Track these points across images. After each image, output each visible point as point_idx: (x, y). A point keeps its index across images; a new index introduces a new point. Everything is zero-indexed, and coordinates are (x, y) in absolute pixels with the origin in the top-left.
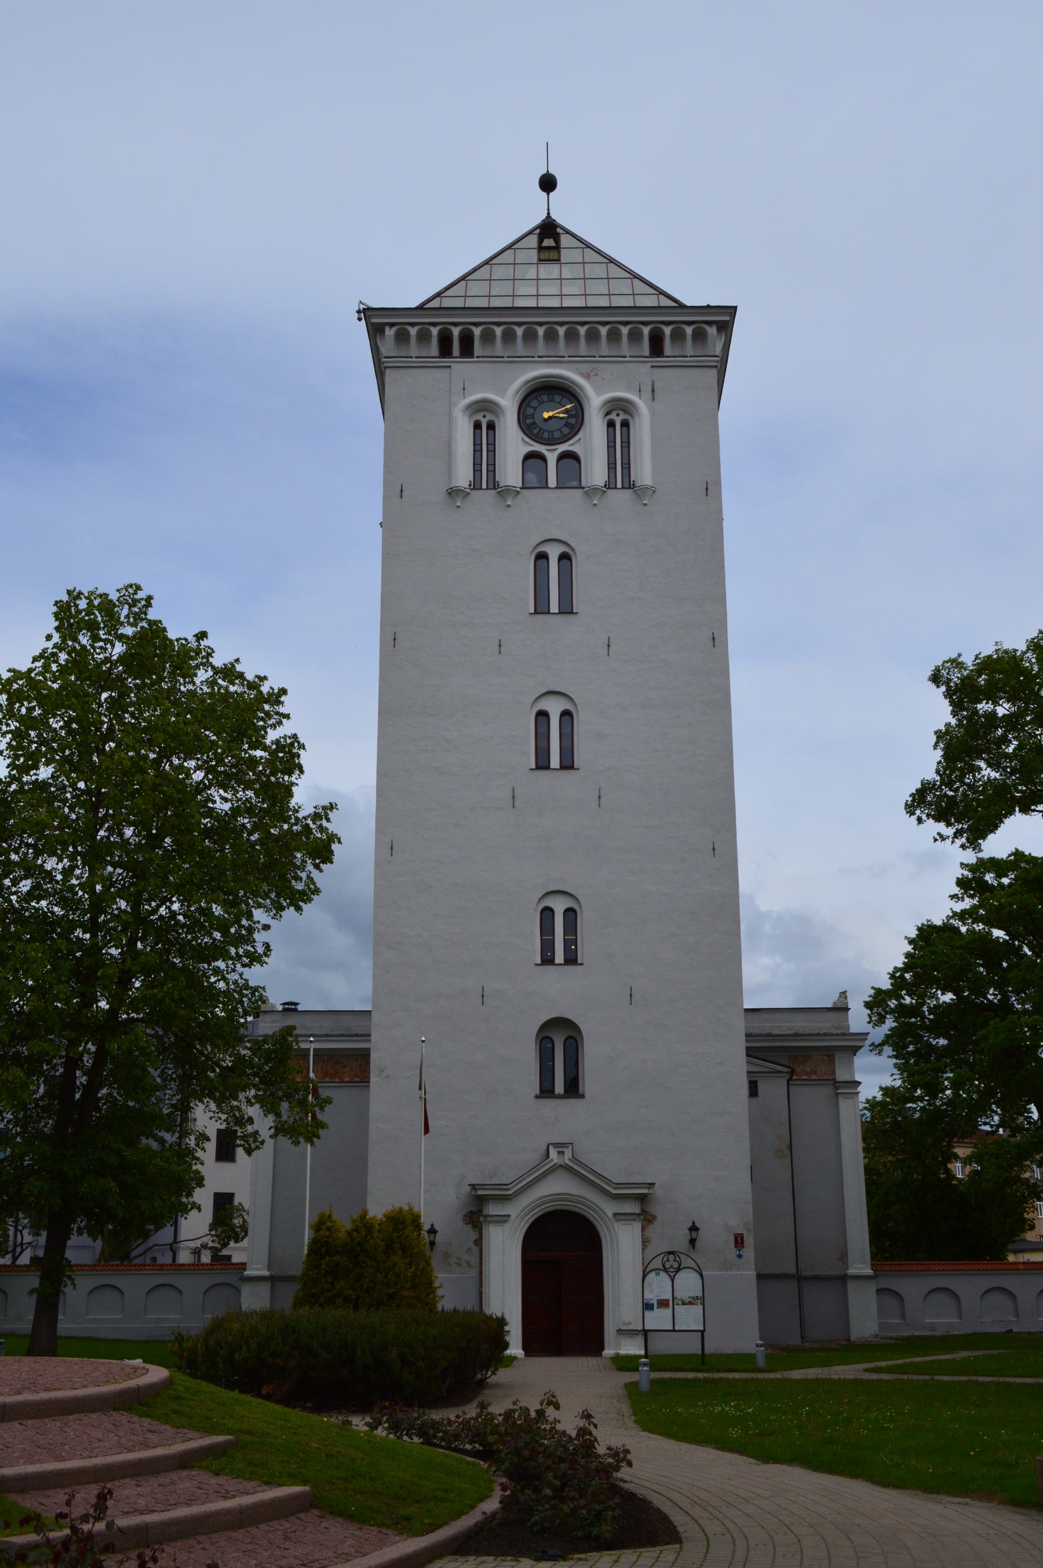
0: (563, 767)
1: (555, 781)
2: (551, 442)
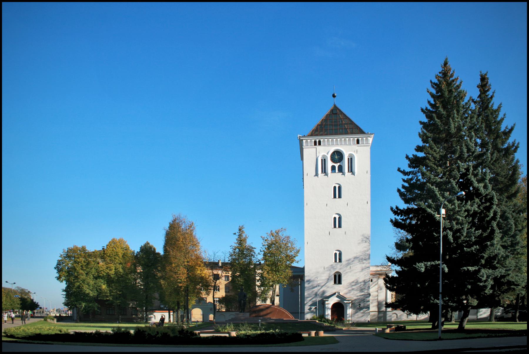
1: (337, 229)
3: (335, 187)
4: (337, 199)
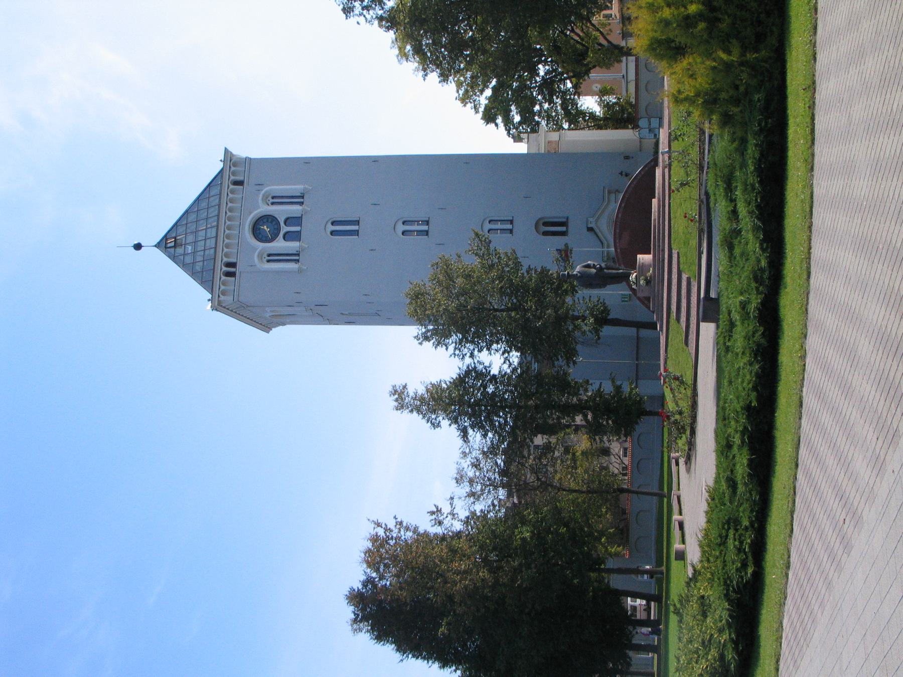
0: (428, 224)
2: (279, 229)
3: (333, 233)
4: (362, 228)
